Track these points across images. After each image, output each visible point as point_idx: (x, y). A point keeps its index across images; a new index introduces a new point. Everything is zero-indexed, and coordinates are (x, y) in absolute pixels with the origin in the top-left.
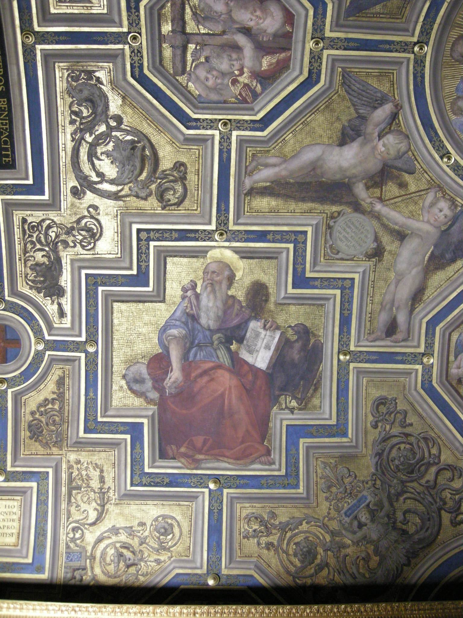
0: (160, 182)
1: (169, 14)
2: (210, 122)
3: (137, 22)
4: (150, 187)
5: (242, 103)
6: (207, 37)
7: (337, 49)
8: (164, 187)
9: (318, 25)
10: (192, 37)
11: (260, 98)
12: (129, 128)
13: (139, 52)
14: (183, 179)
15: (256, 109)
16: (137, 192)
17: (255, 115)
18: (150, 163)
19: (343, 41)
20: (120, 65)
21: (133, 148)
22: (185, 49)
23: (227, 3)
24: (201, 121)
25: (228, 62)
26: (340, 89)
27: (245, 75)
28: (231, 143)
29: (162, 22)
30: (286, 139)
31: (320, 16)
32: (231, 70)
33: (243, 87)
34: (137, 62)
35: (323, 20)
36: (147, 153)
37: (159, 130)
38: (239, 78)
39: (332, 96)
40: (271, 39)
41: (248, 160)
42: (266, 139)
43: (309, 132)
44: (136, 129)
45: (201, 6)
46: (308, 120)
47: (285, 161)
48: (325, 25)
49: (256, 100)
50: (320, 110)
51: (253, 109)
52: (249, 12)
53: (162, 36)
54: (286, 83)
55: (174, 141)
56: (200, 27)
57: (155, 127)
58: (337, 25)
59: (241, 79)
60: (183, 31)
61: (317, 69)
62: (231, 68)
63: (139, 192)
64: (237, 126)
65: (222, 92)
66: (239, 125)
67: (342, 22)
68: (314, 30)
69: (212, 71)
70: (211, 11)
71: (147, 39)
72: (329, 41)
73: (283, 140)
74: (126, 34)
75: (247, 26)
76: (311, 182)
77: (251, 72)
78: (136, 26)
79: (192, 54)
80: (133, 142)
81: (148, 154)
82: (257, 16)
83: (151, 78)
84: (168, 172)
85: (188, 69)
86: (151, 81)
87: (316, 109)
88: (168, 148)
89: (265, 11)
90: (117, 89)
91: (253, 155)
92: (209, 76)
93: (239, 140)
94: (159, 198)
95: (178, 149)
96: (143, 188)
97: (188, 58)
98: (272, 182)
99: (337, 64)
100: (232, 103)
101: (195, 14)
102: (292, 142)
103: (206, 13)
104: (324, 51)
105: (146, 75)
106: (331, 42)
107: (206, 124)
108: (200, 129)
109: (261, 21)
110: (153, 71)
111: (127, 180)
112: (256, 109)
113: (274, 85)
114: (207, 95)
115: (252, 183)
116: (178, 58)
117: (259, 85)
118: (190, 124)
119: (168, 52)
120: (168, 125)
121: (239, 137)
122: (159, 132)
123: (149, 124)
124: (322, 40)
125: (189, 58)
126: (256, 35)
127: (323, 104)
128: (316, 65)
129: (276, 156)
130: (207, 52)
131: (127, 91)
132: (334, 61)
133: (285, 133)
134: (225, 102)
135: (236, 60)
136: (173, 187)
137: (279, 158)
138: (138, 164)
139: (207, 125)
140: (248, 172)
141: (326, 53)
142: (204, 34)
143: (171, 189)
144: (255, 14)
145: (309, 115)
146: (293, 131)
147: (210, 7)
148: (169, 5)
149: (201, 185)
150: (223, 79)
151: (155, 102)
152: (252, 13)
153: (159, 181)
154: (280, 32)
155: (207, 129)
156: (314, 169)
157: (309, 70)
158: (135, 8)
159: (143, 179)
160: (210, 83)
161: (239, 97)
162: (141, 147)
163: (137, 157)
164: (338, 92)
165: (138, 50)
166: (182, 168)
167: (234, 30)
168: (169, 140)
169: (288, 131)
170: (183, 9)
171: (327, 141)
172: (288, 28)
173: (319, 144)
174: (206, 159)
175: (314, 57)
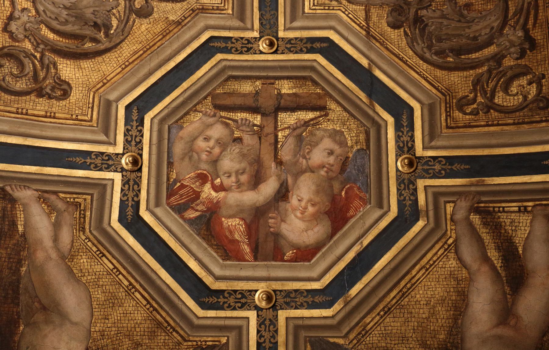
0: (35, 57)
1: (305, 91)
2: (138, 140)
3: (292, 49)
4: (27, 40)
5: (167, 189)
6: (273, 141)
7: (258, 331)
8: (26, 61)
9: (295, 298)
10: (271, 120)
11: (176, 216)
12: (131, 23)
13: (248, 50)
14: (40, 93)
15: (158, 211)
16: (19, 18)
17: (148, 209)
18: (71, 46)
19: (272, 340)
20: (229, 23)
21: (96, 25)
22: (254, 110)
23: (324, 167)
24: (139, 128)
25: (234, 169)
26: (190, 343)
27: (214, 194)
28: (101, 170)
29: (294, 81)
30: (104, 258)
31: (312, 299)
32: (221, 173)
33: (194, 190)
34: (233, 45)
35: (305, 304)
36: (88, 45)
37: (126, 66)
38: (208, 186)
39: (177, 332)
40: (272, 230)
41: (68, 196)
42: (105, 225)
43: (115, 297)
44: (129, 34)
45: (318, 133)
46: (137, 294)
47: (63, 257)
48: (296, 308)
49: (173, 209)
50: (154, 312)
51: (157, 205)
52: (312, 197)
53: (272, 81)
54: (200, 255)
55: (107, 85)
56: (287, 132)
57: (130, 61)
58: (297, 328)
59: (207, 188)
60: (279, 109)
61: (224, 303)
62: (225, 173)
63: (19, 22)
64: (129, 180)
65: (187, 159)
66: (131, 183)
67: (303, 334)
68: (288, 293)
69: (220, 147)
70: (310, 145)
71: (268, 61)
72: (271, 317)
73: (101, 253)
74: (275, 34)
75: (290, 194)
76: (18, 305)
77: (218, 202)
78: (286, 48)
79: (246, 120)
80: (107, 27)
81: (86, 46)
82: (306, 208)
83: (209, 62)
84: (53, 71)
85: (223, 114)
86: (205, 62)
87: (156, 306)
88: (95, 77)
89: (315, 217)
90: (192, 15)
91: (77, 205)
92: (212, 143)
93: (104, 182)
94: (6, 50)
95: (94, 90)
96: (26, 30)
97: (239, 115)
98: (24, 235)
99: (233, 336)
100: (168, 175)
101: (306, 124)
102: (98, 268)
103: (309, 139)
104: (256, 312)
105: (213, 56)
106: (270, 320)
107: (134, 134)
108: (125, 125)
109: (299, 214)
110: (220, 66)
111: (41, 8)
112: (159, 211)
113: (198, 238)
114: (182, 138)
115: (26, 201)
116: (238, 101)
117: (198, 214)
118: (135, 111)
119: (247, 87)
120: (134, 80)
121: (111, 182)
122: (123, 66)
123: (136, 53)
124: (272, 307)
125: (239, 116)
126: (277, 209)
127: (164, 319)
128: (231, 300)
129: (73, 242)
130: (248, 139)
131: (189, 28)
132: (239, 328)
133: (114, 257)
134: (170, 164)
135: (238, 181)
136: (26, 75)
137: (69, 247)
138: (69, 28)
139: (132, 136)
140: (46, 195)
141: (252, 315)
142: (276, 136)
143: (22, 71)
144: (309, 204)
145: (146, 295)
146: (118, 270)
147: (317, 144)
148: (318, 91)
149: (27, 119)
150: (206, 162)
151: (172, 64)
152: (310, 201)
153: (38, 55)
154: (283, 242)
155: (125, 135)
156: (44, 308)
157: (223, 291)
158: (312, 47)
159: (42, 33)
160: (201, 143)
161: (178, 184)
162: (98, 36)
163: (81, 29)
164: (185, 341)
165: (251, 48)
166: (59, 93)
167: (283, 177)
168: (108, 78)
169: (118, 261)
170: (313, 109)
171: (97, 329)
172: (289, 254)
173: (92, 316)
174: (73, 130)
175: (244, 296)
